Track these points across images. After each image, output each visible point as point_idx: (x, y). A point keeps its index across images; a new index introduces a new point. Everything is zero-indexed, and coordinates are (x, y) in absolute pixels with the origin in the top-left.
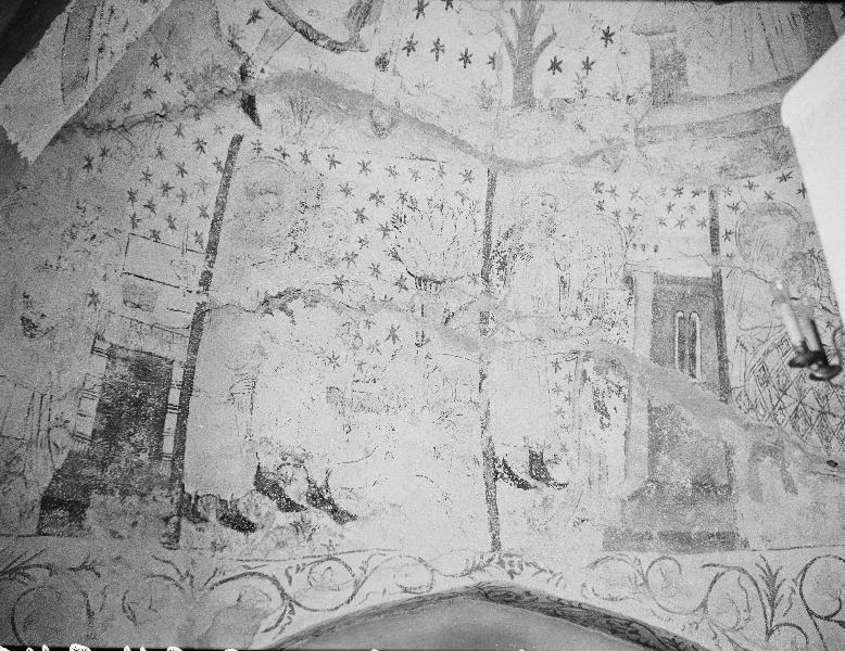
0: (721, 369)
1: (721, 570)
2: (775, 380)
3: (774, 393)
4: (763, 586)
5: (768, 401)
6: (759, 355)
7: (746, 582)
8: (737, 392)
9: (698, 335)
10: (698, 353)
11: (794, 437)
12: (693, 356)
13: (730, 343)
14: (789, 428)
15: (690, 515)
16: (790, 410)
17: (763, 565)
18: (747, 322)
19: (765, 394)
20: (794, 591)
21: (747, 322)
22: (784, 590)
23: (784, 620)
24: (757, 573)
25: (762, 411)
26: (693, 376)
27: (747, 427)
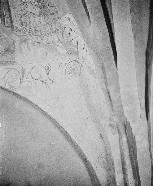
0: (11, 22)
1: (10, 69)
2: (24, 24)
3: (24, 27)
4: (21, 72)
5: (23, 29)
6: (20, 18)
7: (16, 72)
8: (16, 28)
9: (5, 15)
10: (5, 19)
11: (30, 37)
12: (4, 20)
13: (13, 16)
14: (28, 35)
15: (3, 57)
16: (29, 31)
17: (22, 68)
18: (16, 10)
19: (22, 27)
20: (29, 73)
21: (16, 10)
22: (27, 73)
23: (26, 80)
24: (19, 70)
25: (22, 32)
26: (5, 25)
27: (18, 36)
